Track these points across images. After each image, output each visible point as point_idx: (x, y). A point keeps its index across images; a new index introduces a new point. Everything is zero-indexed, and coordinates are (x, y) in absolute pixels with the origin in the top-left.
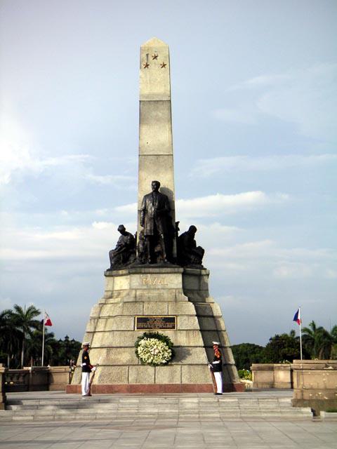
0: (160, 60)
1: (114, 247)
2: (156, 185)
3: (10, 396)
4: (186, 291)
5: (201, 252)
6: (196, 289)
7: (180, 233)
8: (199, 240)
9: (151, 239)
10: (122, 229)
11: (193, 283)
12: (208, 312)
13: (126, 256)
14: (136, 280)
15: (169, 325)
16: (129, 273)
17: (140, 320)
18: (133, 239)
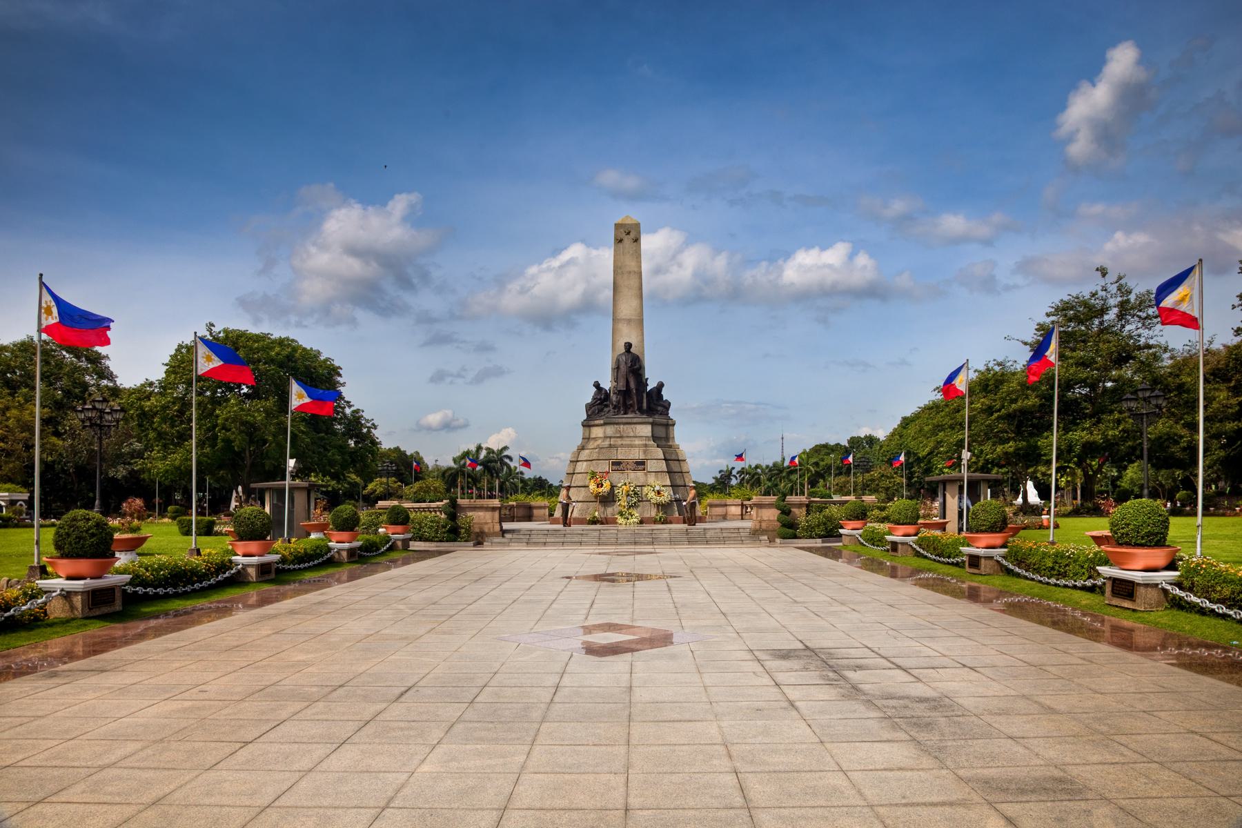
0: (632, 235)
1: (589, 400)
2: (628, 346)
3: (506, 526)
4: (655, 438)
5: (667, 406)
6: (663, 437)
7: (649, 388)
8: (666, 394)
9: (625, 393)
10: (597, 385)
11: (661, 432)
12: (674, 457)
13: (602, 406)
14: (610, 430)
15: (641, 467)
16: (605, 424)
17: (613, 464)
18: (607, 395)
